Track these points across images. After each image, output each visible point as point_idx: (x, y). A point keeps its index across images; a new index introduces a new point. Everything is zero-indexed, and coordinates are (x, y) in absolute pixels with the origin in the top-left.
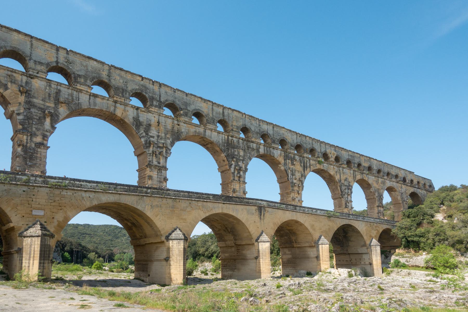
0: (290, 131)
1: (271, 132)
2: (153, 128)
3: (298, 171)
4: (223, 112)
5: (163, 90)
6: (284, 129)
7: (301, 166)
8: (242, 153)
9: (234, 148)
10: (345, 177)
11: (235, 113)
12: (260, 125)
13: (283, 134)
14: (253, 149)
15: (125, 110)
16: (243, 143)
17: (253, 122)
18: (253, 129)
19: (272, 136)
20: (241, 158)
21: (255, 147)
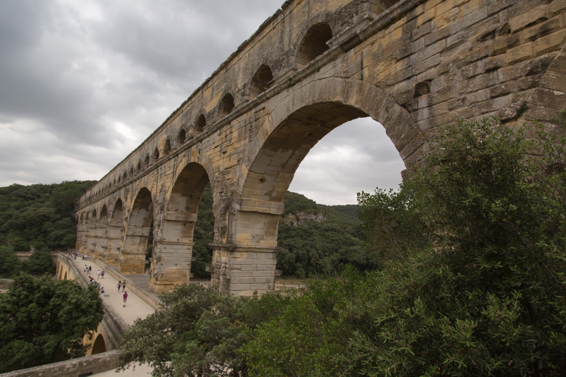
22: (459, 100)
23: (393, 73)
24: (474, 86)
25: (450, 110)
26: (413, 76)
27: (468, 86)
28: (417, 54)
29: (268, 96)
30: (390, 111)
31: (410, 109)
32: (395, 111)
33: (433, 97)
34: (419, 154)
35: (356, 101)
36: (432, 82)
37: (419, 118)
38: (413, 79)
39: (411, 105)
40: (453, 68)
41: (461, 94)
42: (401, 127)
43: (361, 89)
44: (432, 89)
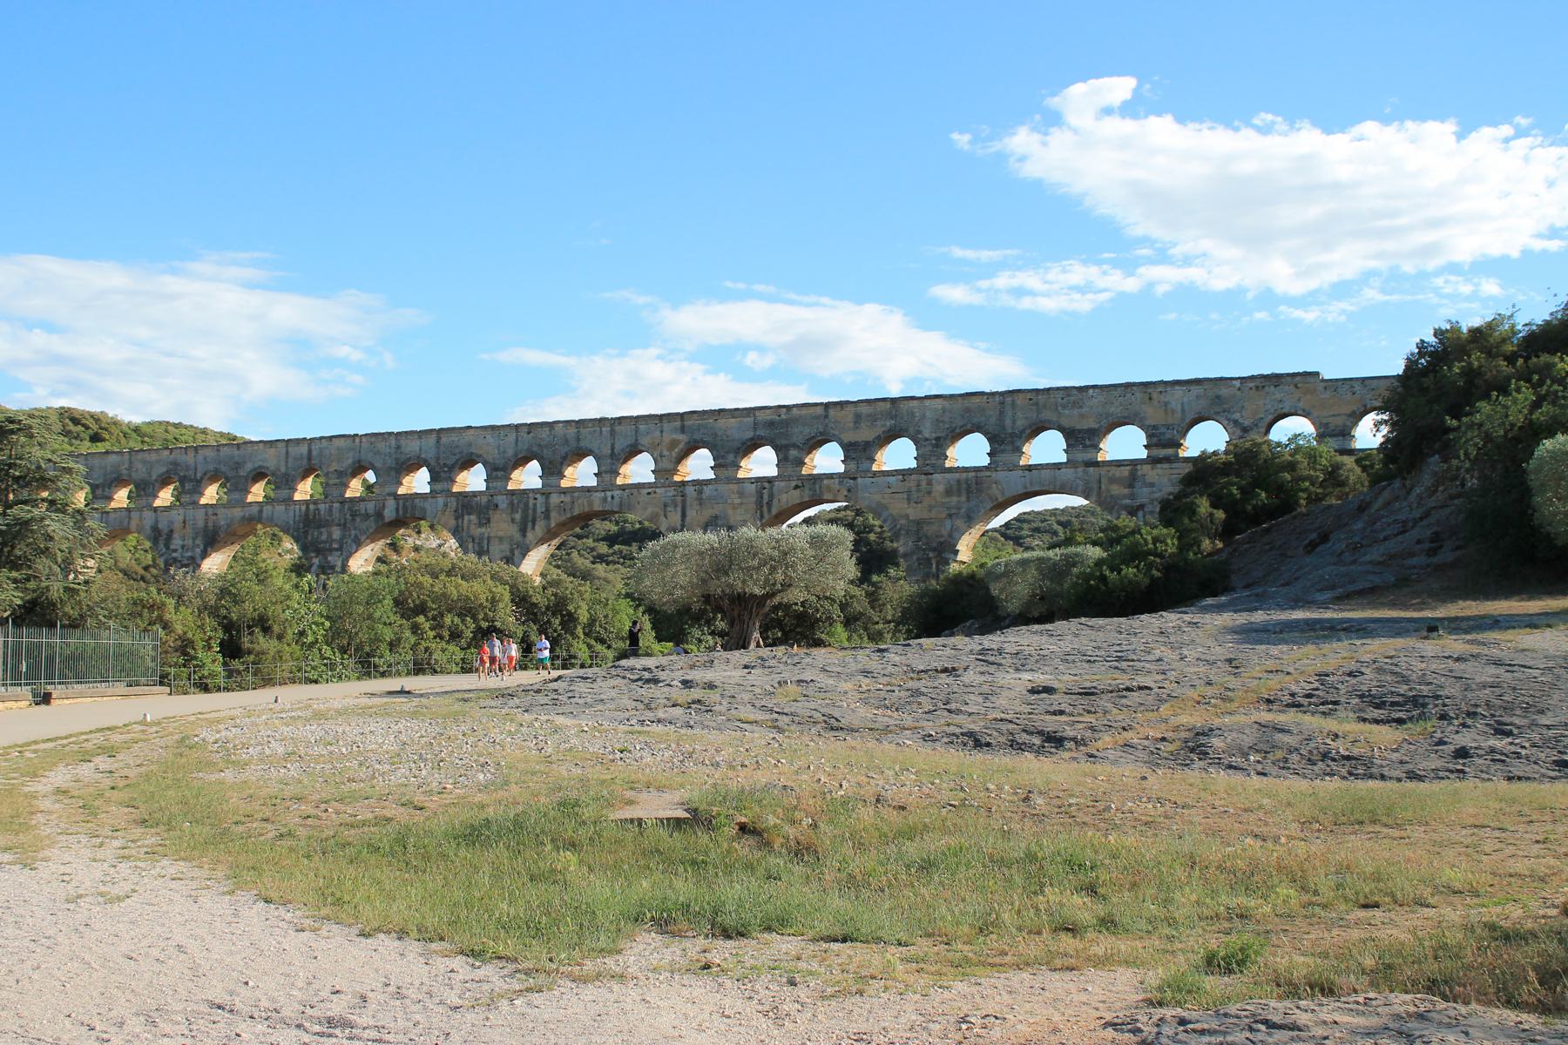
0: (493, 427)
1: (429, 455)
2: (176, 535)
3: (501, 539)
4: (310, 451)
5: (200, 457)
6: (472, 432)
7: (513, 521)
8: (336, 533)
9: (319, 527)
10: (708, 513)
11: (336, 441)
12: (398, 447)
13: (470, 445)
14: (367, 516)
15: (141, 519)
16: (341, 510)
17: (381, 446)
18: (378, 465)
19: (433, 463)
20: (335, 546)
21: (371, 511)
43: (1099, 494)
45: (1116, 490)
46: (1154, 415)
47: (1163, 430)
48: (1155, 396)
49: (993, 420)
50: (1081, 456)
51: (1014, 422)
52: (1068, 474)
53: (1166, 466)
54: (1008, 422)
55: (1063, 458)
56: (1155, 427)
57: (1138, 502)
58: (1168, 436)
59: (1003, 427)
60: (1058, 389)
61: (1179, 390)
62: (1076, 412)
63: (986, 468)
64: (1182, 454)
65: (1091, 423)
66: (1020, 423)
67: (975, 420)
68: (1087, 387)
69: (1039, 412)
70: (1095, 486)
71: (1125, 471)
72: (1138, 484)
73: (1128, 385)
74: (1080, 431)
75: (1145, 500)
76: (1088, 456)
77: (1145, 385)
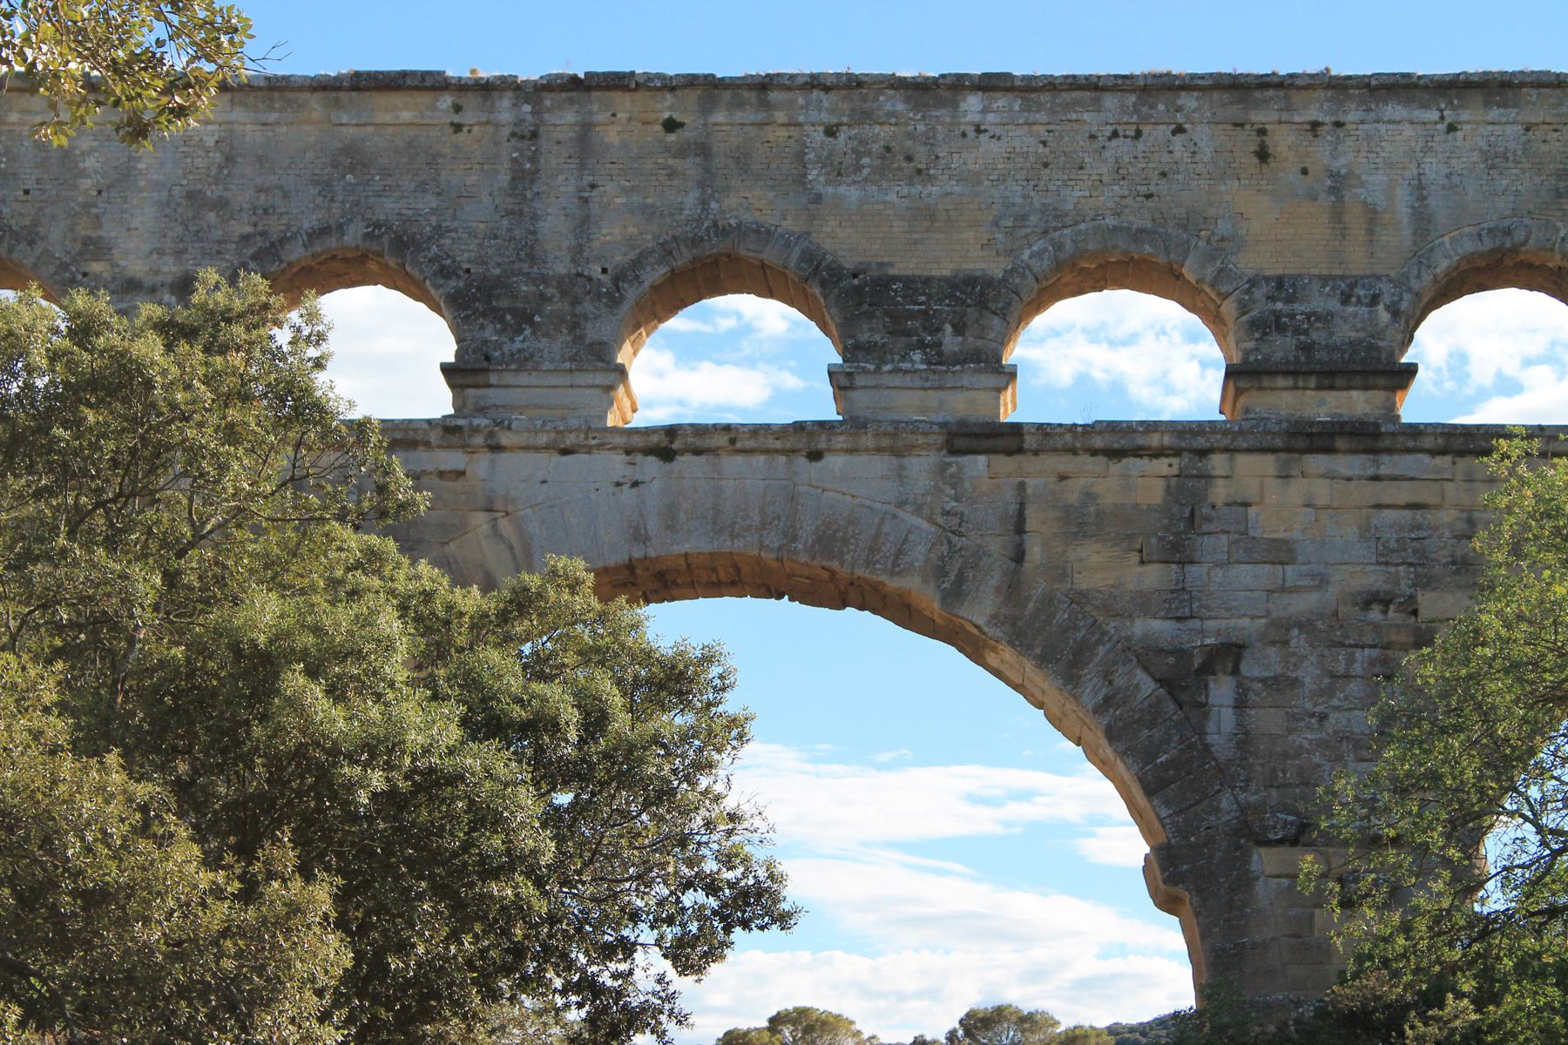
22: (1312, 715)
23: (1131, 587)
24: (1346, 698)
25: (1290, 731)
26: (1192, 617)
27: (1329, 692)
28: (1204, 568)
29: (505, 439)
30: (1119, 682)
31: (1185, 697)
32: (1137, 686)
33: (1249, 689)
34: (1209, 813)
35: (995, 616)
36: (1247, 653)
37: (1211, 727)
38: (1190, 624)
39: (1185, 688)
40: (1298, 640)
41: (1316, 705)
42: (1157, 734)
43: (1013, 588)
44: (1245, 668)
45: (1100, 568)
46: (1274, 231)
47: (1320, 302)
48: (1283, 141)
49: (480, 213)
50: (909, 399)
51: (584, 225)
52: (856, 479)
53: (1348, 464)
54: (554, 226)
55: (824, 407)
56: (1283, 287)
57: (1214, 629)
58: (1344, 332)
59: (530, 252)
60: (815, 83)
61: (1401, 129)
62: (894, 194)
63: (447, 429)
64: (1414, 407)
65: (964, 252)
66: (616, 235)
67: (388, 208)
68: (958, 85)
69: (708, 183)
70: (997, 546)
71: (1149, 482)
72: (1213, 545)
73: (1159, 89)
74: (913, 285)
75: (1245, 626)
76: (959, 404)
77: (1240, 89)
